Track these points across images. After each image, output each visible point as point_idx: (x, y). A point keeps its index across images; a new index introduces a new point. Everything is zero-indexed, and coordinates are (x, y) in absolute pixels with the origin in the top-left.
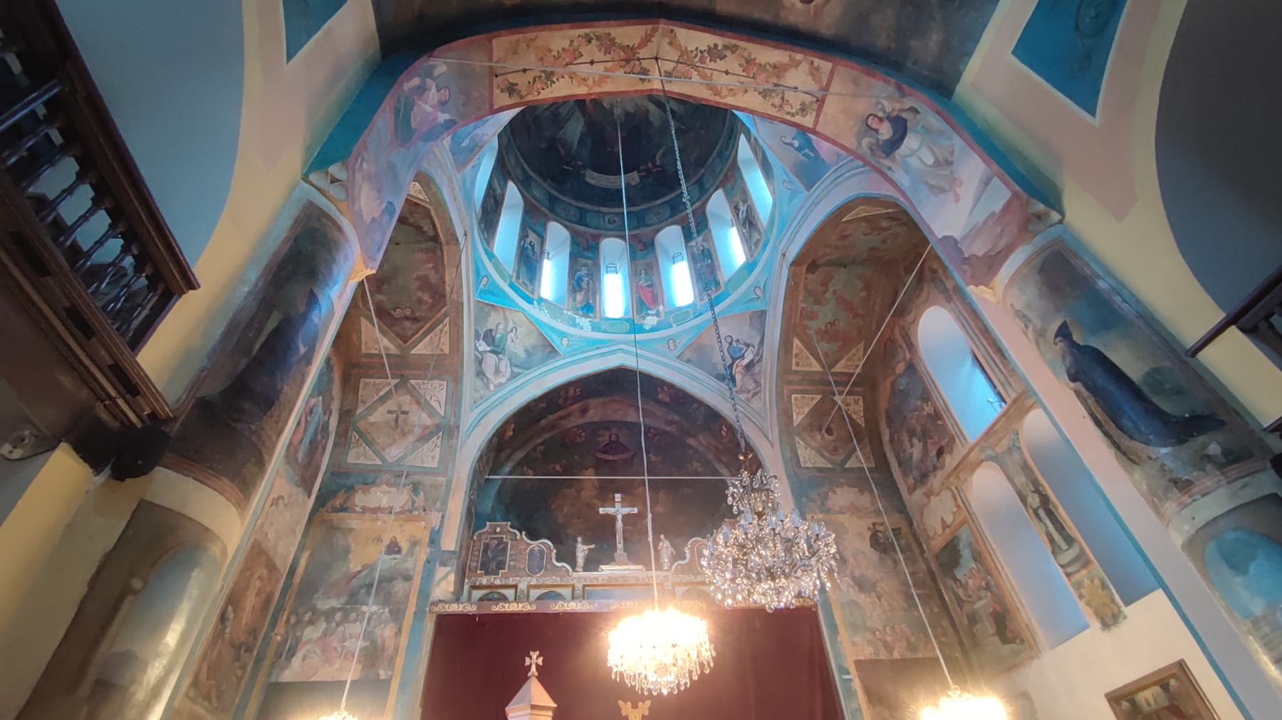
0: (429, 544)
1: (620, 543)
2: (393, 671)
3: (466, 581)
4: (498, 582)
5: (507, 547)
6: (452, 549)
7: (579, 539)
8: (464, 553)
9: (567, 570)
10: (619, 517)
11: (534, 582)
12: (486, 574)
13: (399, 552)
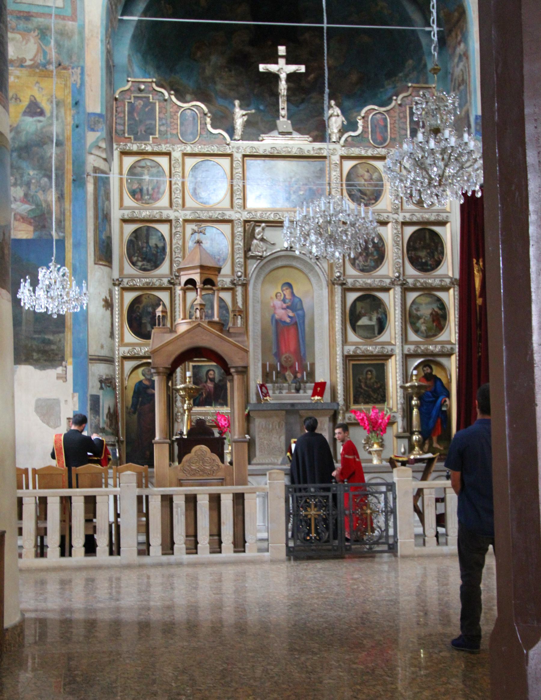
0: (73, 106)
1: (283, 109)
2: (64, 233)
3: (115, 146)
4: (149, 149)
5: (153, 110)
6: (98, 110)
7: (237, 103)
8: (109, 115)
9: (224, 138)
10: (283, 76)
11: (189, 150)
12: (135, 139)
13: (42, 113)
